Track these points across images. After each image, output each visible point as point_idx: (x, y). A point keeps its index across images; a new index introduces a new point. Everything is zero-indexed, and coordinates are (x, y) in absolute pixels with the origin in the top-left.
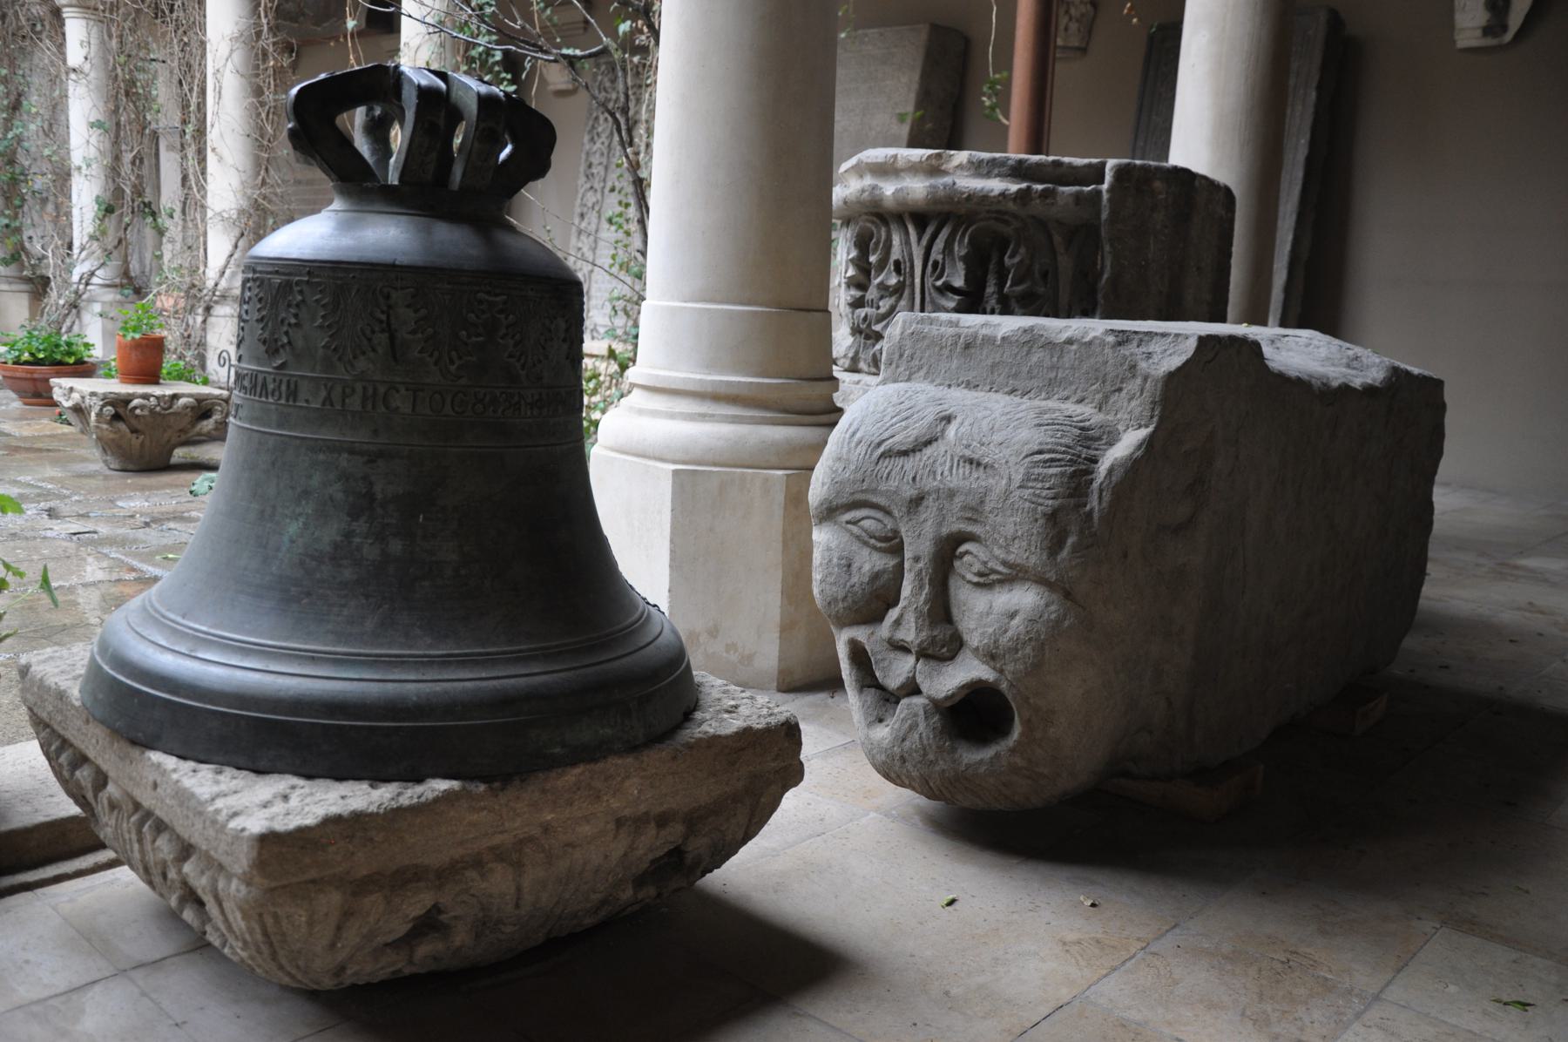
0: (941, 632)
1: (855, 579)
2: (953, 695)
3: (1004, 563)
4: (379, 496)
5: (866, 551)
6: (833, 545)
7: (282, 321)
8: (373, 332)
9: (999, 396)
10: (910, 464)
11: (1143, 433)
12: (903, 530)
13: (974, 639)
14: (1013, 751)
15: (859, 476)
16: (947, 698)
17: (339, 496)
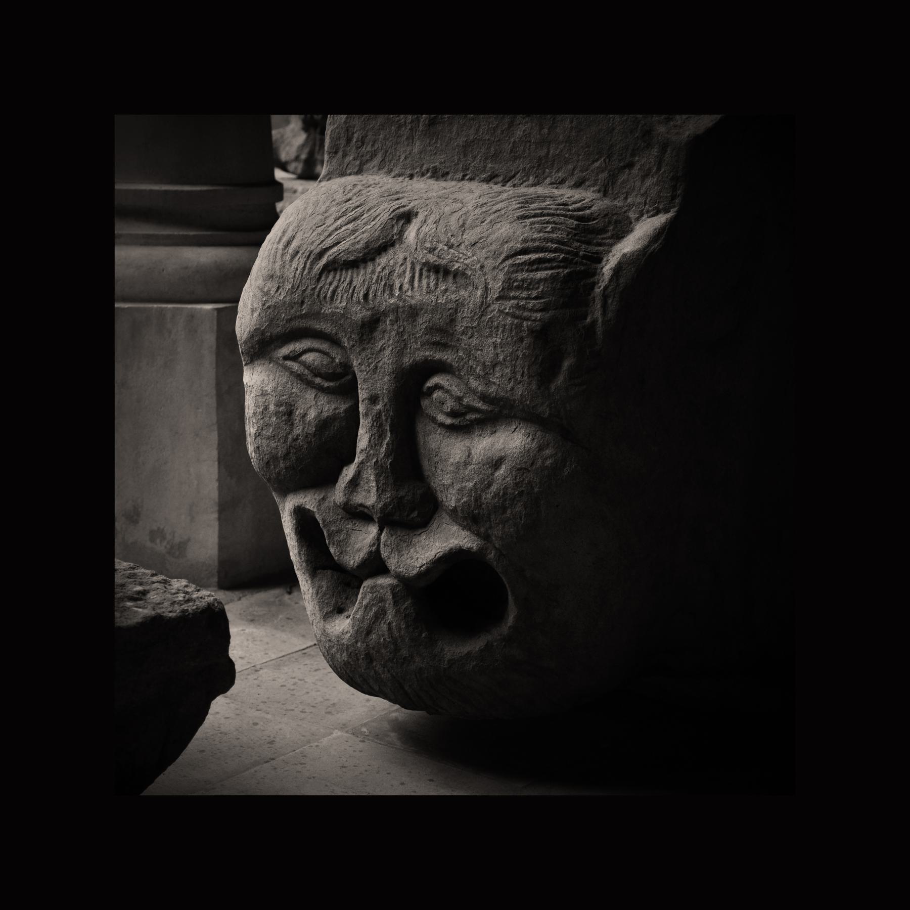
1: (298, 431)
2: (428, 571)
3: (484, 397)
5: (310, 395)
6: (269, 389)
9: (474, 185)
10: (360, 278)
11: (660, 220)
12: (355, 363)
13: (451, 499)
15: (296, 297)
16: (420, 575)
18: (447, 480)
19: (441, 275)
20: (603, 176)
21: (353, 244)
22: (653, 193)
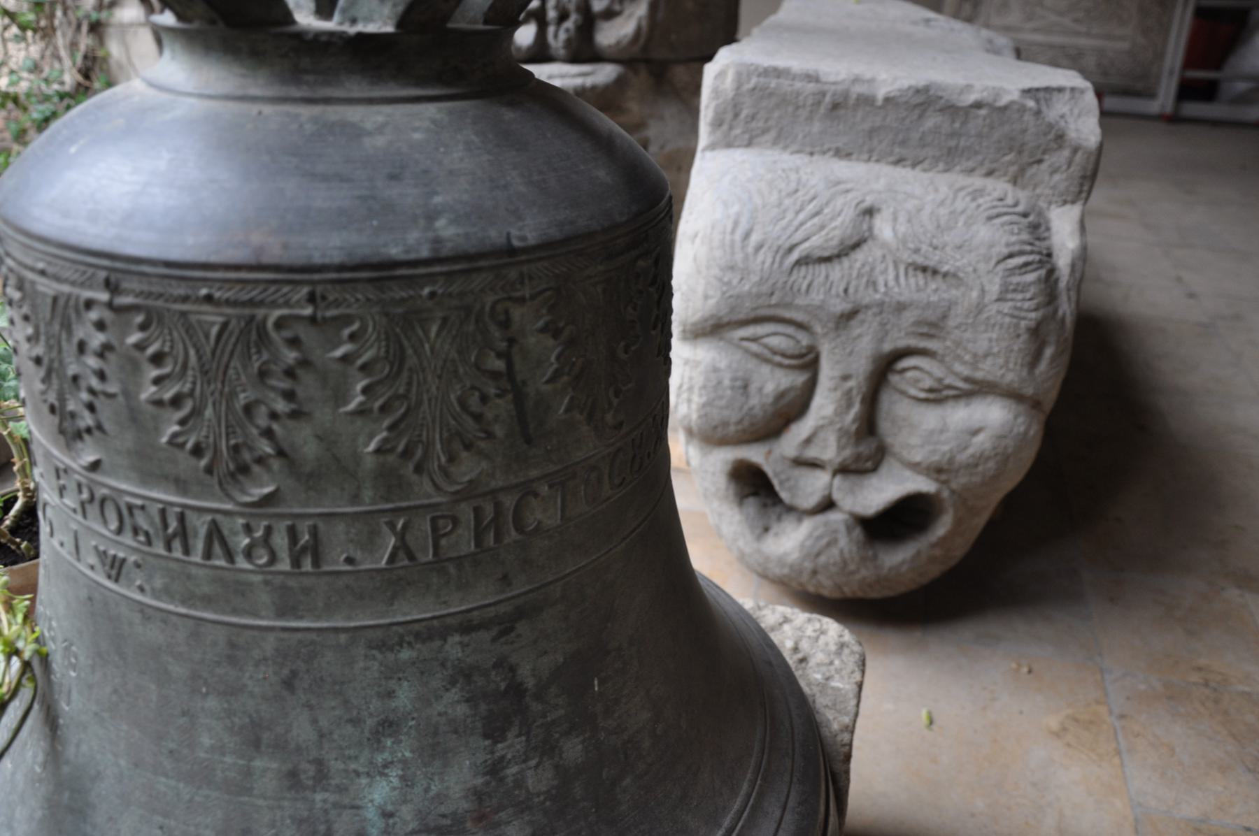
0: (866, 448)
1: (754, 401)
4: (530, 683)
5: (766, 369)
7: (248, 409)
8: (484, 399)
10: (836, 272)
14: (933, 546)
15: (765, 288)
17: (462, 710)
18: (915, 440)
19: (929, 274)
20: (1013, 169)
21: (827, 241)
22: (1062, 187)
